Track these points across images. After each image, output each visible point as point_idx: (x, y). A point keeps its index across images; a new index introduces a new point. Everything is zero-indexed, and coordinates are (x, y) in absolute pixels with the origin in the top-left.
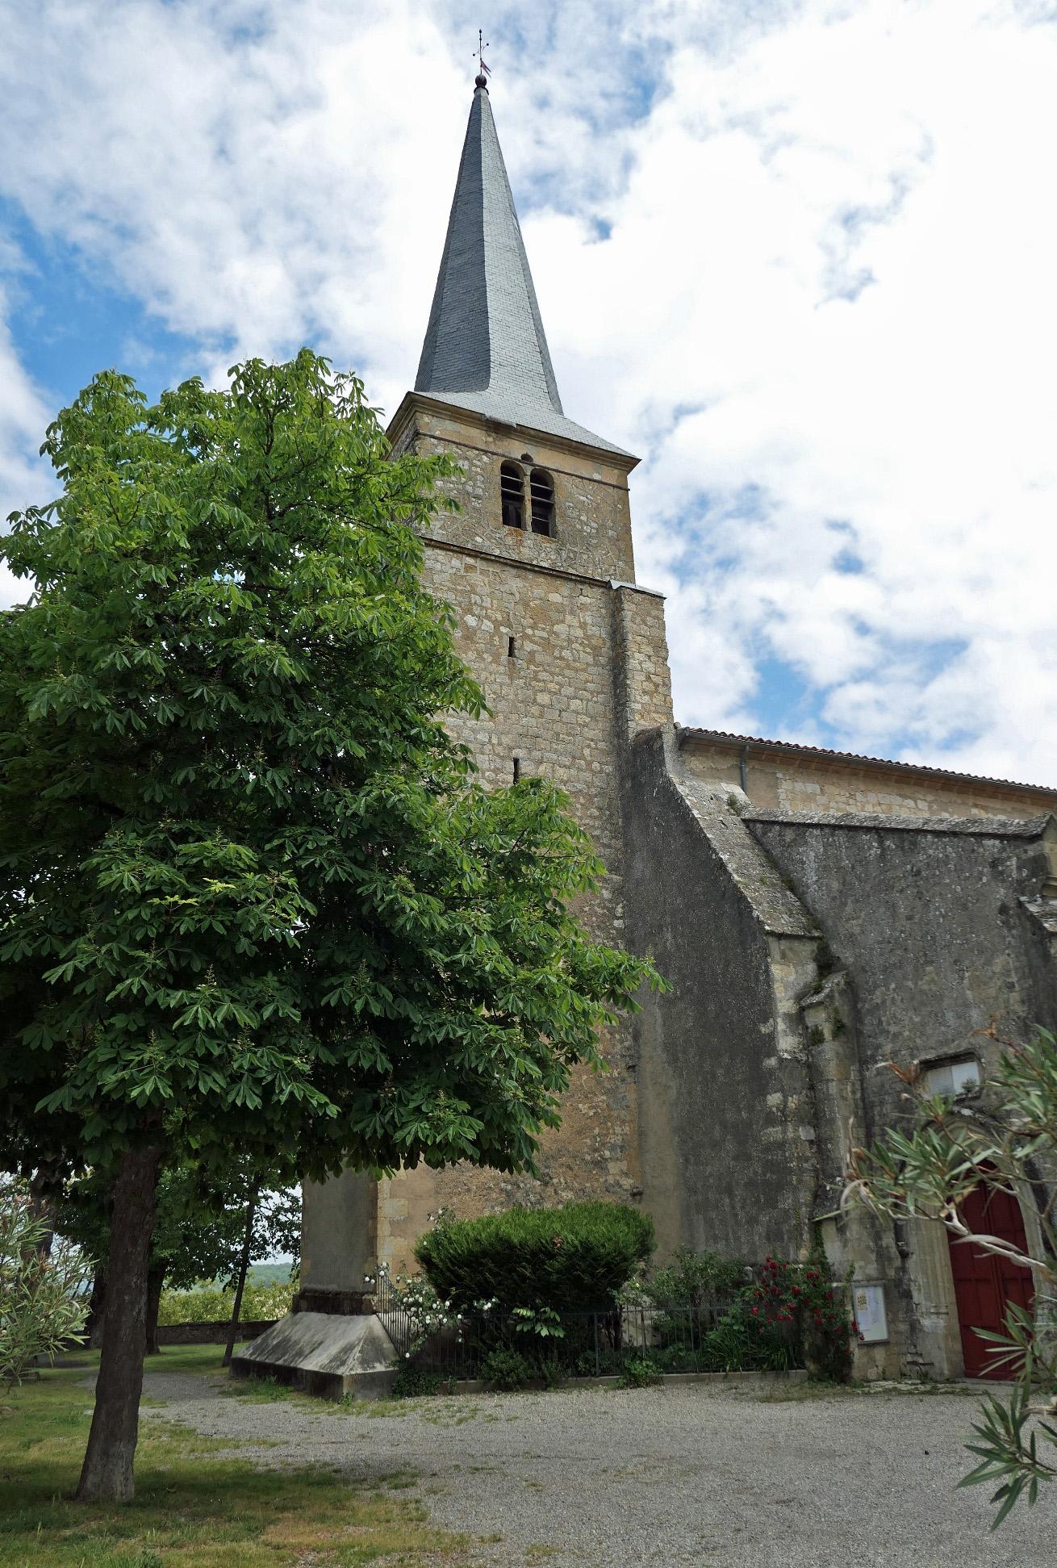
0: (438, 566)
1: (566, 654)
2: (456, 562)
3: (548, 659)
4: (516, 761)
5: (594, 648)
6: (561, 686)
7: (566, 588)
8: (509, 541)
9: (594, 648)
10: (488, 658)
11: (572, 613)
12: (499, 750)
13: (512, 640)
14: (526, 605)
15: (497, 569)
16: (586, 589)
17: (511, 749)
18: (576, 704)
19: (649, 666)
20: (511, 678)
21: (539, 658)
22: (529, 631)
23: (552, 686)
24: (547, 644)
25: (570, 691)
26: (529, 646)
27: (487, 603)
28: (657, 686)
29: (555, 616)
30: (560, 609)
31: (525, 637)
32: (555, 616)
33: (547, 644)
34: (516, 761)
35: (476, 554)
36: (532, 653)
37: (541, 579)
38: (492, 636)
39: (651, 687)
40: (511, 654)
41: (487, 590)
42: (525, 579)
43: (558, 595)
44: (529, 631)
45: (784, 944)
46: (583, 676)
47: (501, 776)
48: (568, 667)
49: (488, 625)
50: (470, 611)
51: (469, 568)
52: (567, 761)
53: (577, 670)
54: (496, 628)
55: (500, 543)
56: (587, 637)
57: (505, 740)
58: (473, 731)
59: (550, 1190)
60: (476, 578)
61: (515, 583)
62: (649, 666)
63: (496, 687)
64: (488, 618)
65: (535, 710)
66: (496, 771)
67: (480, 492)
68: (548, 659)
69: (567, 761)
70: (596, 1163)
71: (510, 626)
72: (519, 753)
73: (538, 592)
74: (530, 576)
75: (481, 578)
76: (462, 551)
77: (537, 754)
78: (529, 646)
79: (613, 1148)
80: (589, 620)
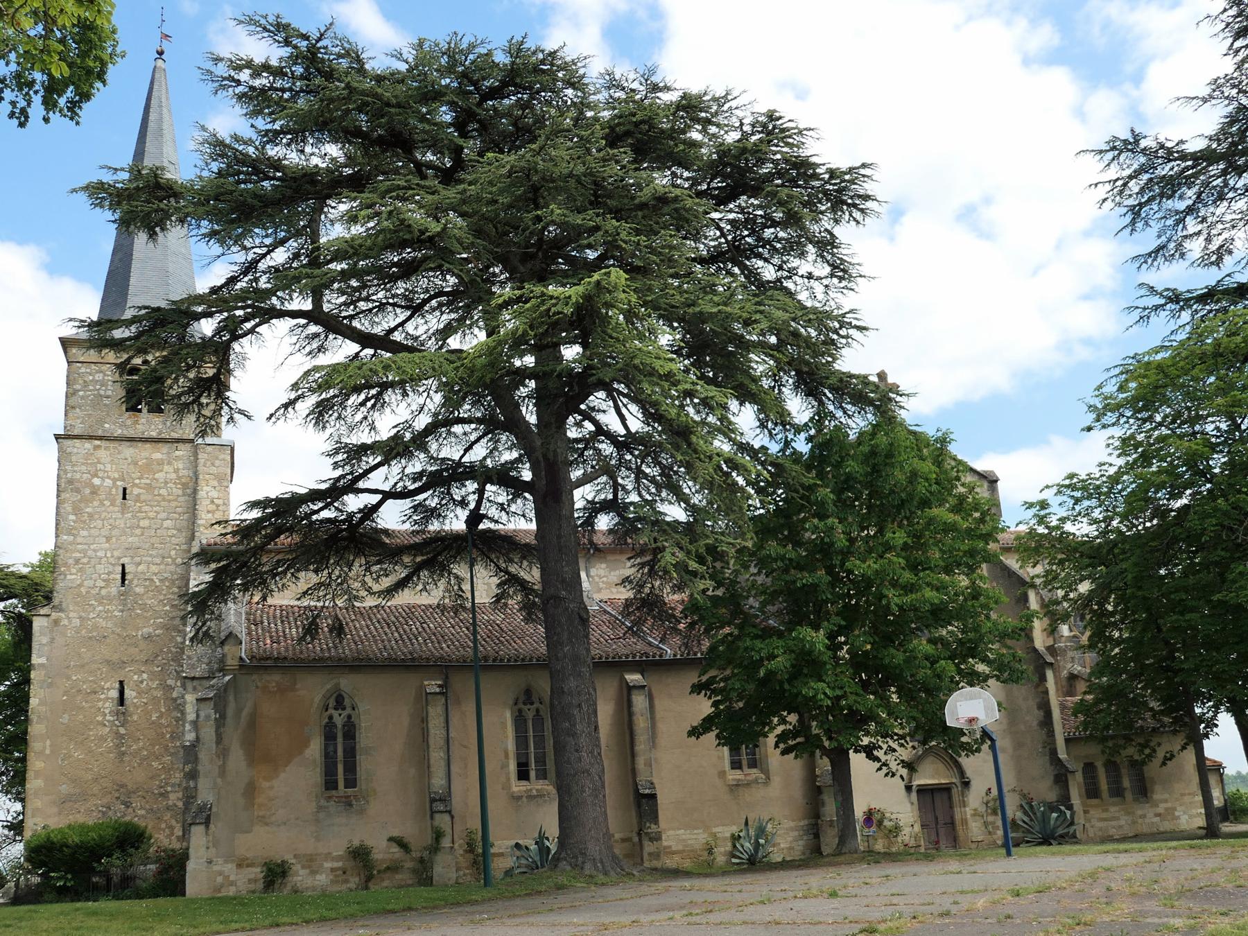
0: (75, 450)
1: (163, 492)
2: (88, 445)
3: (150, 497)
4: (123, 566)
5: (183, 484)
6: (158, 513)
7: (165, 448)
8: (129, 422)
9: (183, 484)
10: (107, 503)
11: (169, 463)
12: (112, 560)
13: (125, 489)
14: (136, 464)
15: (116, 444)
16: (180, 446)
17: (119, 558)
18: (168, 523)
19: (214, 494)
20: (123, 513)
21: (143, 497)
22: (137, 481)
23: (152, 515)
24: (149, 488)
25: (164, 515)
26: (136, 491)
27: (108, 467)
28: (218, 506)
29: (155, 467)
30: (160, 463)
31: (135, 485)
32: (155, 467)
33: (149, 488)
34: (123, 566)
35: (101, 438)
36: (138, 495)
37: (148, 445)
38: (111, 489)
39: (214, 507)
40: (124, 498)
41: (109, 459)
42: (136, 447)
43: (159, 453)
44: (137, 481)
45: (195, 683)
46: (174, 504)
47: (112, 576)
48: (164, 500)
49: (108, 482)
50: (96, 476)
51: (98, 447)
52: (158, 560)
53: (169, 501)
54: (114, 483)
55: (123, 425)
56: (179, 478)
57: (116, 554)
58: (95, 551)
59: (130, 810)
60: (102, 454)
61: (128, 451)
62: (214, 494)
63: (111, 521)
64: (109, 477)
65: (138, 531)
66: (109, 573)
67: (110, 393)
68: (150, 497)
69: (158, 560)
70: (161, 795)
71: (123, 480)
72: (125, 560)
73: (145, 454)
74: (140, 444)
75: (105, 453)
76: (91, 438)
77: (138, 559)
78: (136, 491)
79: (173, 785)
80: (181, 466)
